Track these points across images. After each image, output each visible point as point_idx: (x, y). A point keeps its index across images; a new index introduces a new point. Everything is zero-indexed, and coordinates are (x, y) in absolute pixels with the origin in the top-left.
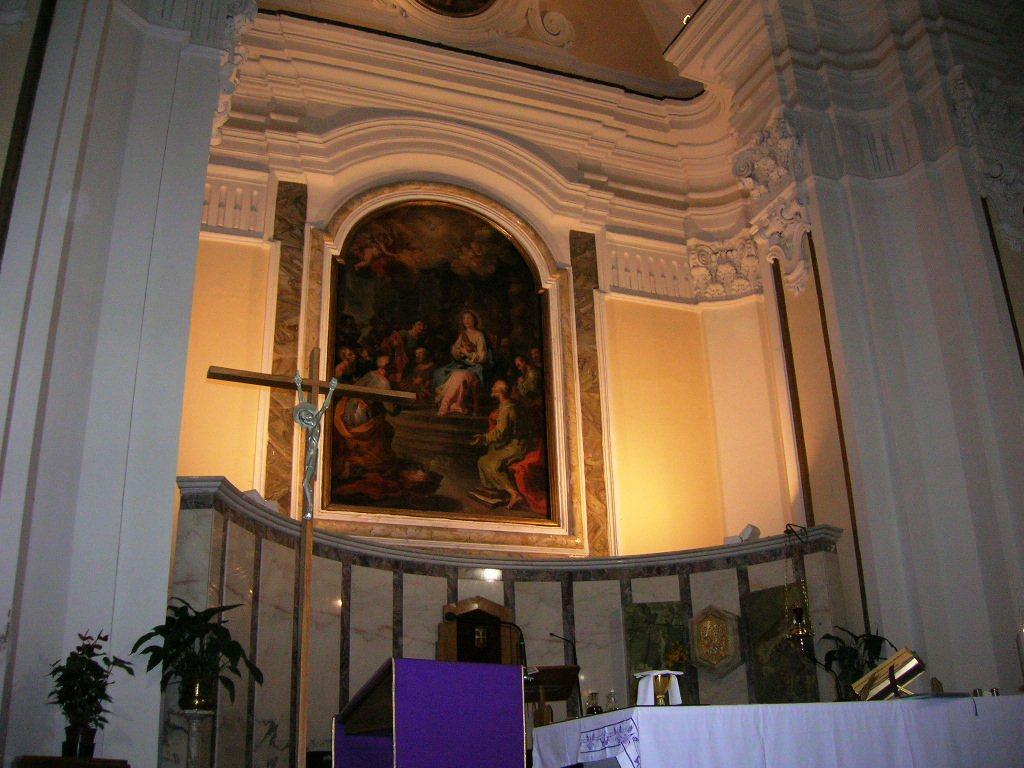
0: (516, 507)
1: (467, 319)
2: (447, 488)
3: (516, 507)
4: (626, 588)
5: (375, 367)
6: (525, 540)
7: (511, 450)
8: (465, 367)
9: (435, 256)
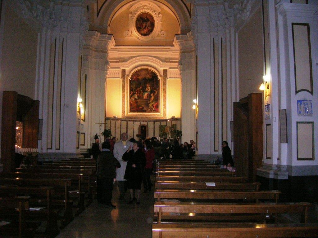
0: (154, 110)
1: (148, 85)
2: (145, 109)
3: (154, 110)
4: (161, 122)
5: (135, 94)
6: (154, 115)
7: (154, 103)
8: (147, 92)
9: (143, 77)
